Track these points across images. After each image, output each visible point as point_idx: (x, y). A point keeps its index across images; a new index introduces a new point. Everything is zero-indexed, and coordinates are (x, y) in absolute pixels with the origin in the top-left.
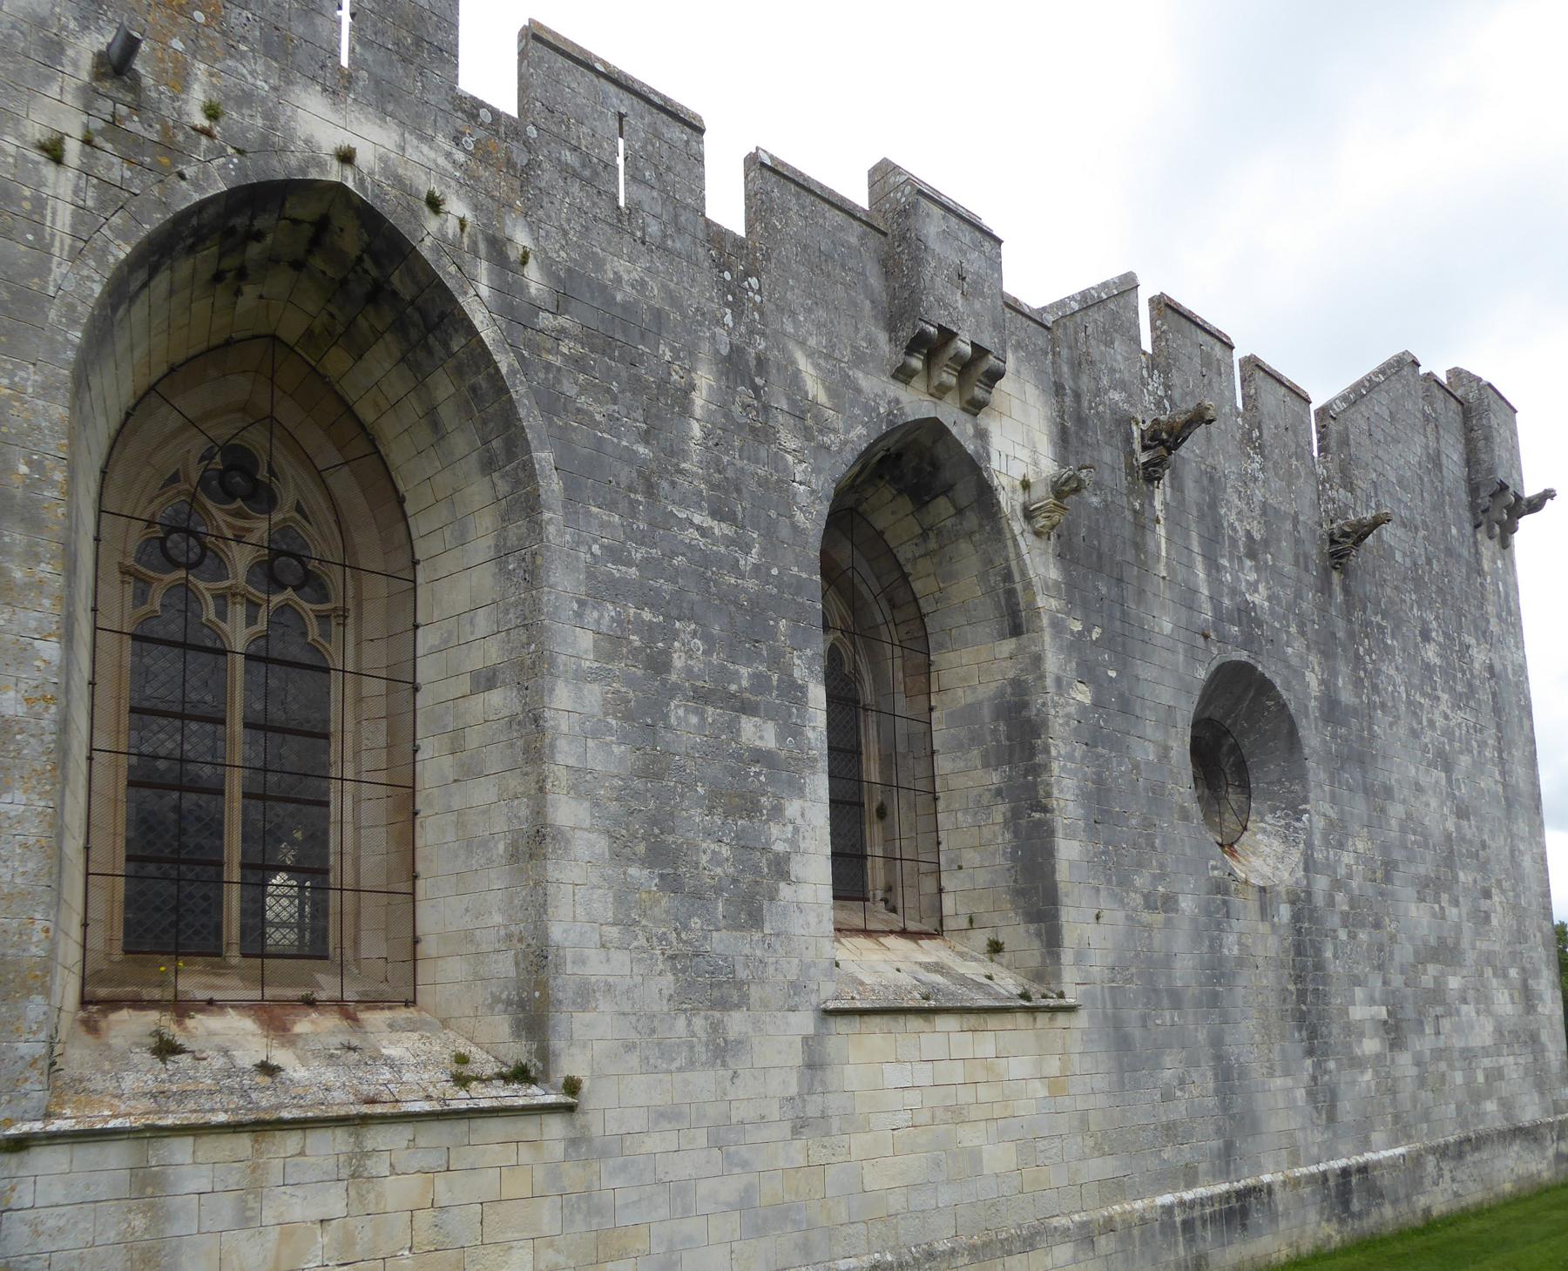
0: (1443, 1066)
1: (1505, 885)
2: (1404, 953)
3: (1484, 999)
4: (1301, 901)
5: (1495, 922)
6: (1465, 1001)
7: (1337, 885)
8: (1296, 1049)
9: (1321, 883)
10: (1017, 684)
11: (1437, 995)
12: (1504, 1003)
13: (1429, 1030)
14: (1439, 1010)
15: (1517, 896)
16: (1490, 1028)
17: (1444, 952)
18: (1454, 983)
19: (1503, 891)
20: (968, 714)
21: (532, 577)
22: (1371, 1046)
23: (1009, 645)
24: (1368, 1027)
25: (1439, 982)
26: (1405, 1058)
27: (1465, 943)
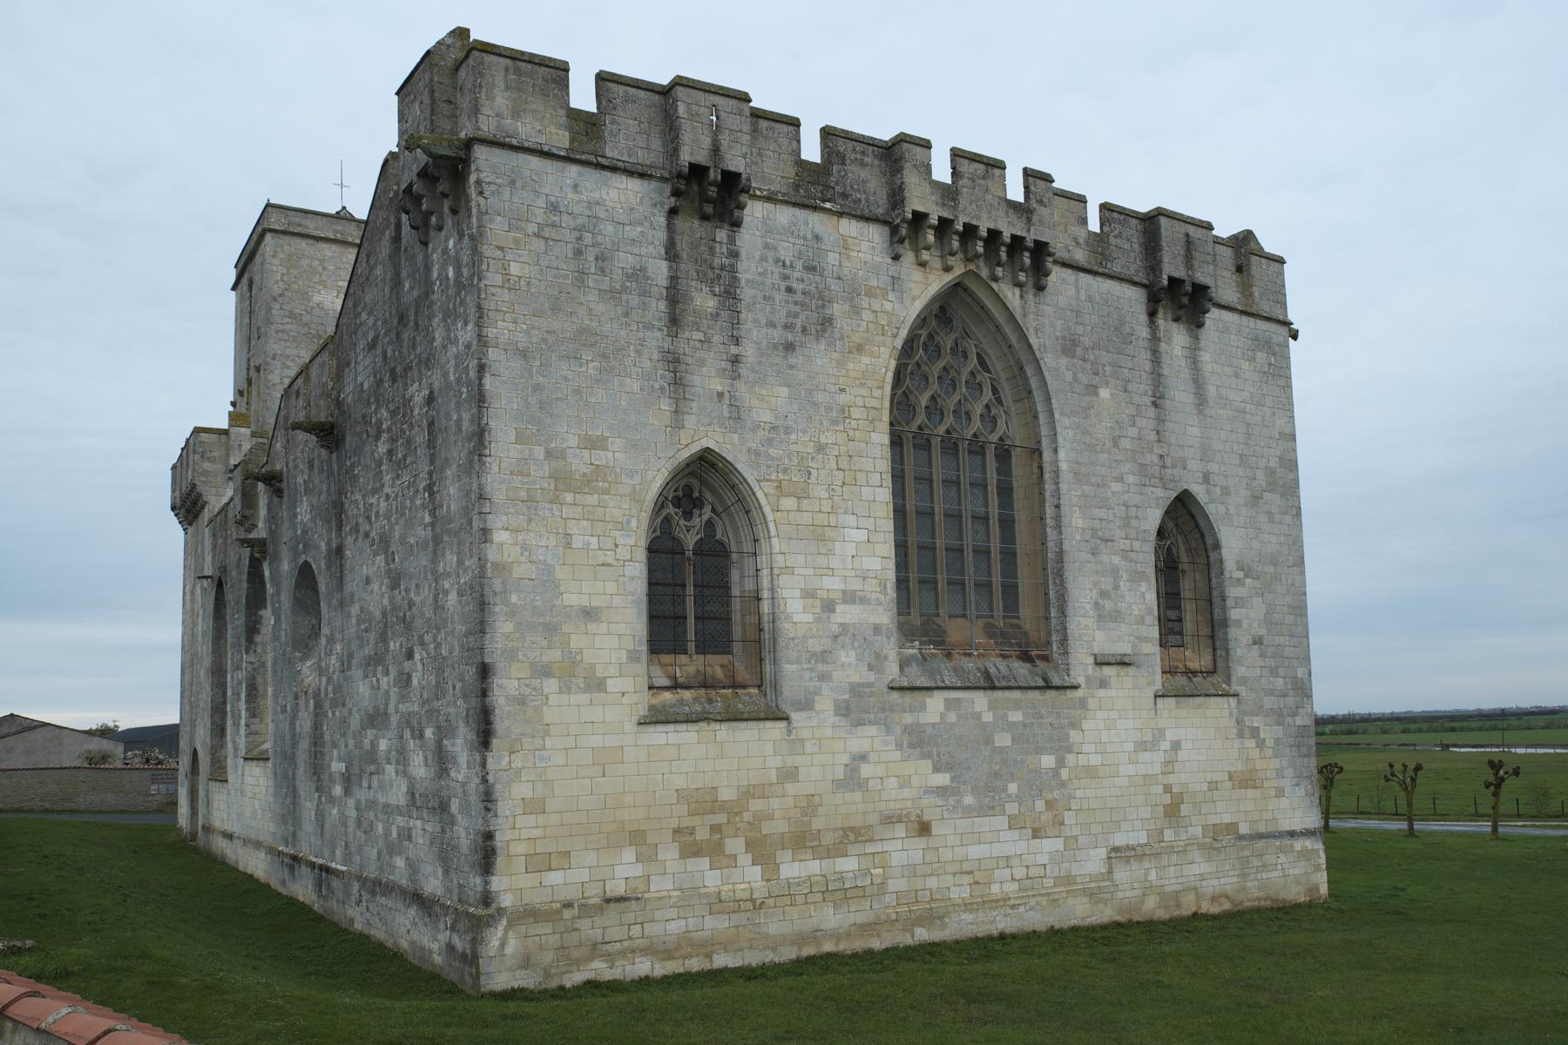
0: (372, 814)
1: (427, 638)
3: (403, 759)
5: (415, 681)
6: (389, 762)
8: (313, 786)
11: (371, 756)
12: (420, 768)
13: (365, 784)
14: (372, 768)
15: (438, 646)
16: (404, 789)
18: (383, 745)
19: (423, 644)
22: (338, 790)
24: (337, 776)
25: (374, 744)
26: (351, 803)
27: (391, 710)
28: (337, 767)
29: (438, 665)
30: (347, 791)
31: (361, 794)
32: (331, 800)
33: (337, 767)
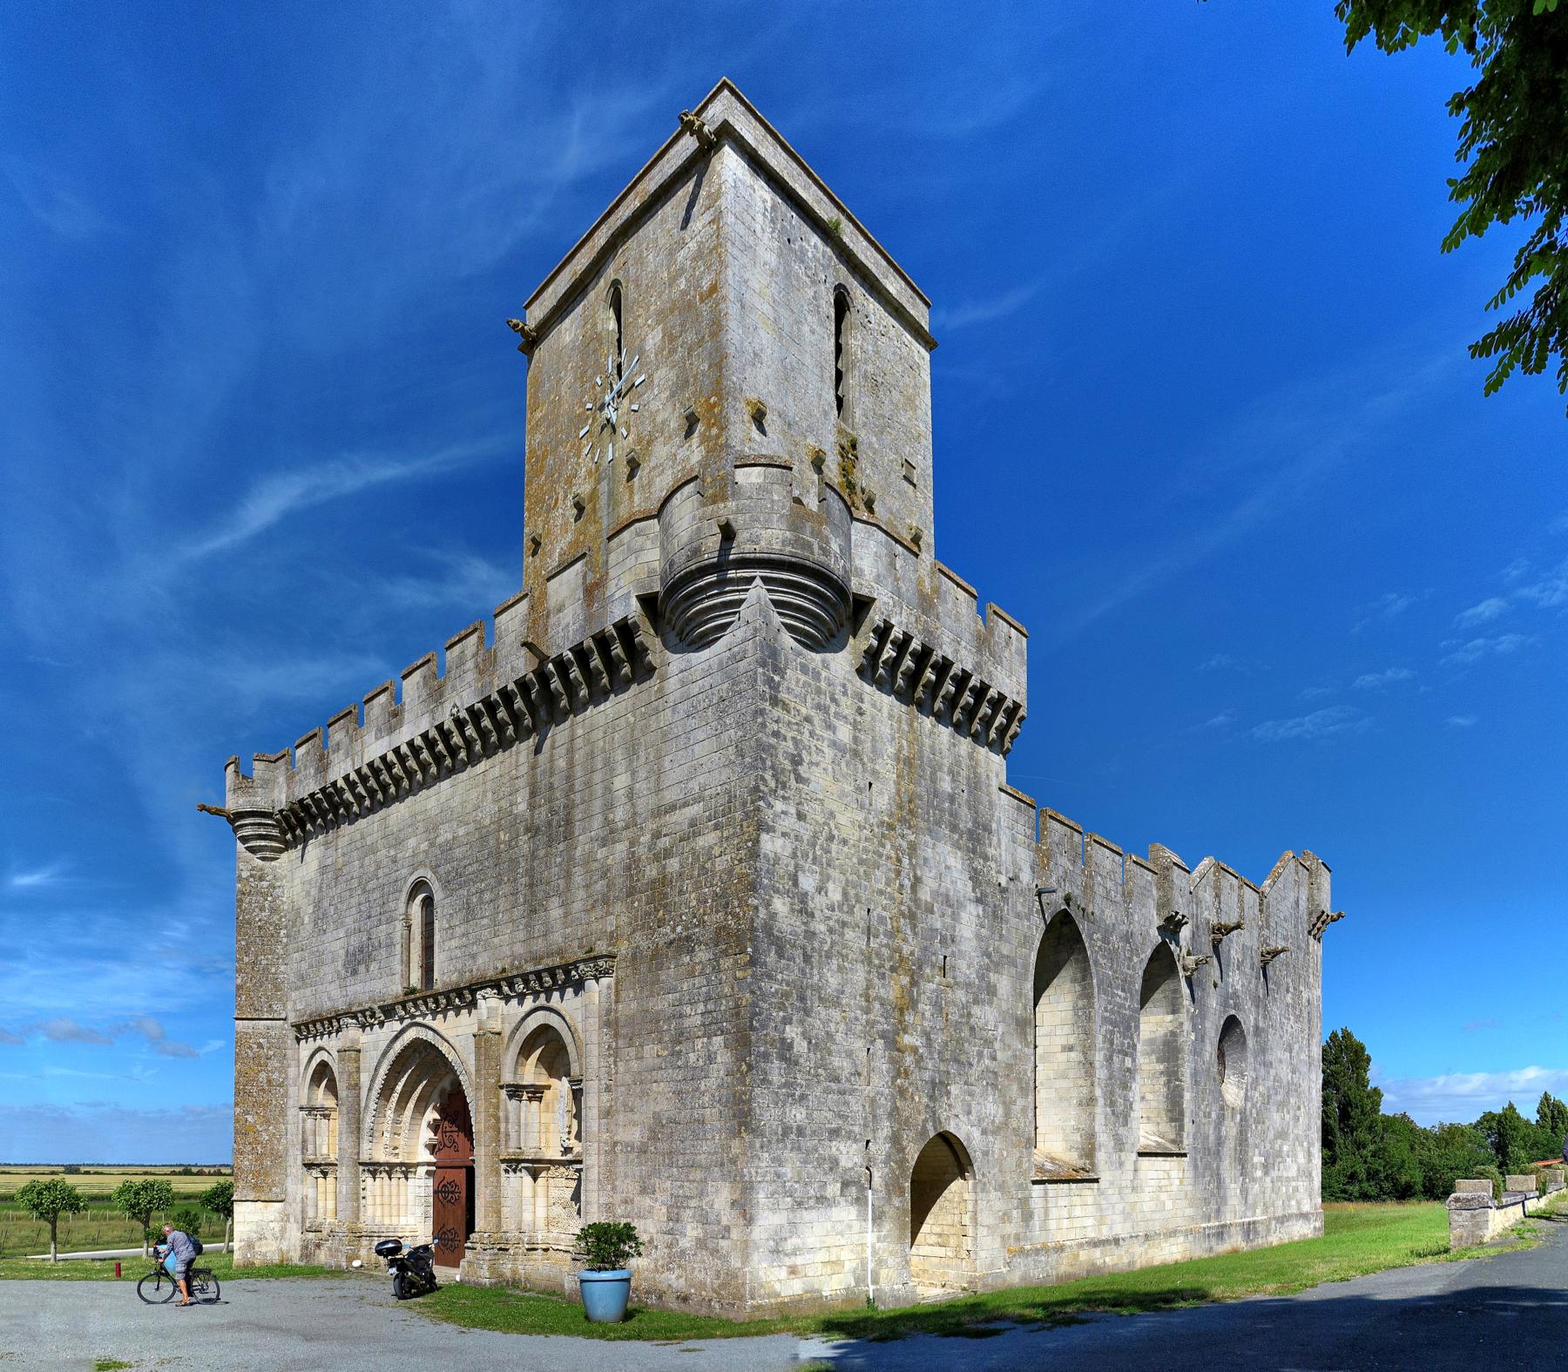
2: (1271, 1135)
4: (1243, 1112)
7: (1254, 1106)
9: (1249, 1105)
10: (1173, 1034)
11: (1279, 1154)
17: (1282, 1135)
18: (1285, 1148)
20: (1151, 1042)
21: (1089, 1018)
23: (1170, 1017)
28: (1258, 1159)
29: (1309, 1115)
30: (1266, 1173)
31: (1274, 1174)
32: (1254, 1180)
33: (1258, 1159)
